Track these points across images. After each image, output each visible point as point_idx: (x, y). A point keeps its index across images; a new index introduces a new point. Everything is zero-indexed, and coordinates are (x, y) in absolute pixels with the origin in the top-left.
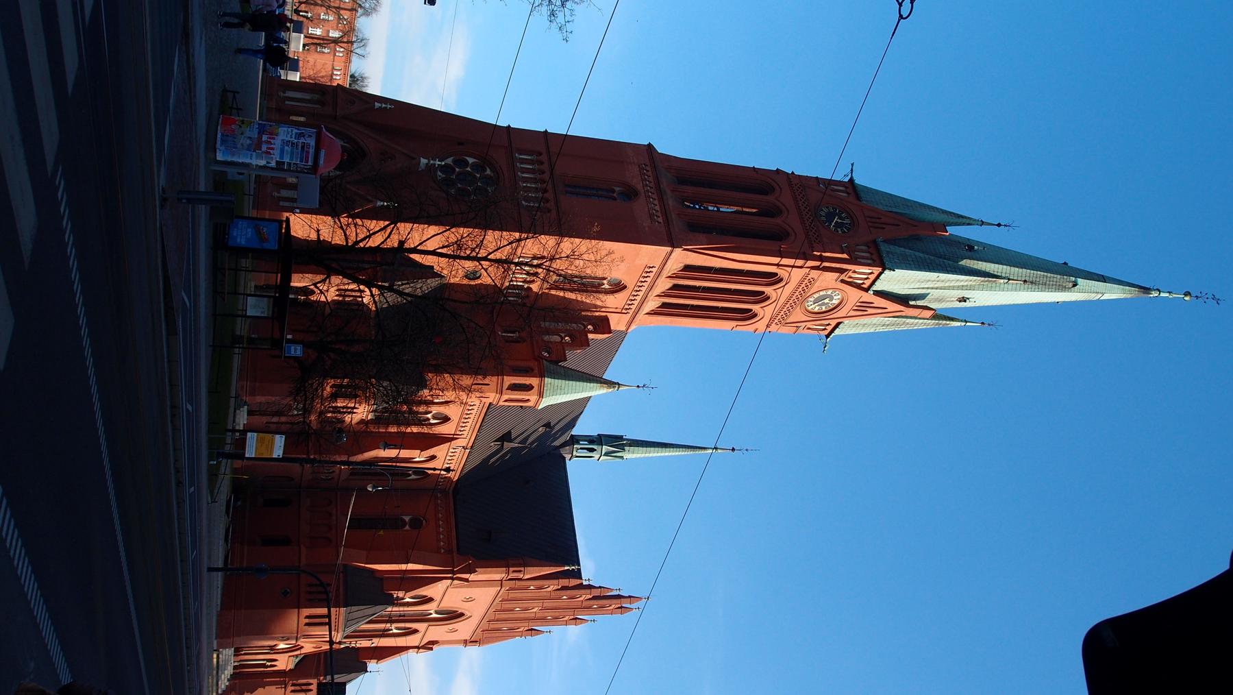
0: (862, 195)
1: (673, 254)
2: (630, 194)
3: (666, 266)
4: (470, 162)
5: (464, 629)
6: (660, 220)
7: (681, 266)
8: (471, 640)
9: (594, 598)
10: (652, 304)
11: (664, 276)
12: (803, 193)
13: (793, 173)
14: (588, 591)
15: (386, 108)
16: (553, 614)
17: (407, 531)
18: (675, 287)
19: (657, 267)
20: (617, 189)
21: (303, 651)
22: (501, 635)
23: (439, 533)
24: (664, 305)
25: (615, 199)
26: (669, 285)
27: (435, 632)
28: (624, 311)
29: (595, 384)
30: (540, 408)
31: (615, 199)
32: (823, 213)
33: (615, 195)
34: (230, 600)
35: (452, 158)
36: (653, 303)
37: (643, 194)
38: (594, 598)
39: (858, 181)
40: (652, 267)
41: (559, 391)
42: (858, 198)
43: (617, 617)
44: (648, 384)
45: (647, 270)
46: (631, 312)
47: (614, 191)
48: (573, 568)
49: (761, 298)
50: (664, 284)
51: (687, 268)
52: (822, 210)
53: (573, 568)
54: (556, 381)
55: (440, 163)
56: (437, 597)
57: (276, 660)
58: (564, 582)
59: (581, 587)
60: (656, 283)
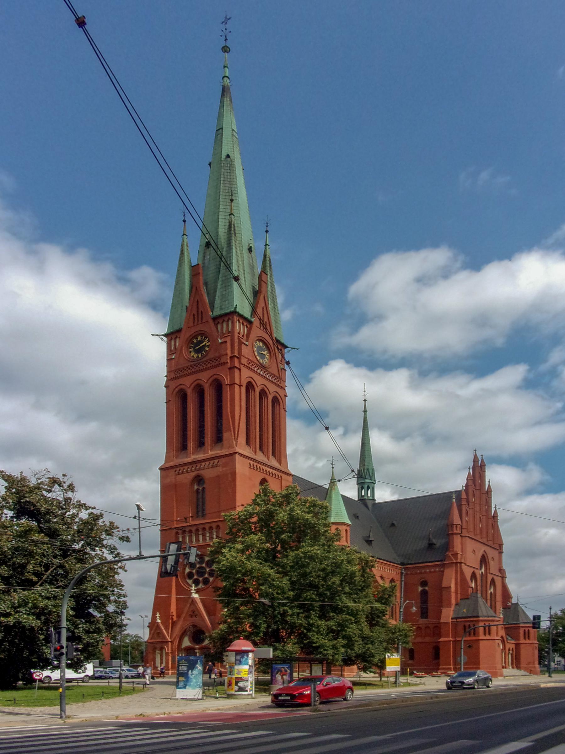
0: (176, 328)
1: (240, 452)
2: (199, 479)
3: (248, 456)
6: (216, 461)
7: (247, 447)
10: (275, 463)
11: (255, 456)
18: (261, 449)
19: (250, 461)
20: (196, 487)
24: (274, 454)
25: (203, 489)
26: (261, 453)
28: (280, 478)
29: (333, 493)
30: (351, 523)
31: (203, 489)
32: (195, 356)
33: (201, 488)
36: (273, 461)
37: (198, 472)
39: (165, 331)
40: (250, 464)
41: (339, 513)
42: (179, 331)
44: (331, 462)
45: (252, 467)
46: (280, 474)
47: (198, 490)
49: (263, 393)
50: (260, 457)
51: (248, 442)
52: (193, 356)
54: (332, 515)
60: (261, 461)
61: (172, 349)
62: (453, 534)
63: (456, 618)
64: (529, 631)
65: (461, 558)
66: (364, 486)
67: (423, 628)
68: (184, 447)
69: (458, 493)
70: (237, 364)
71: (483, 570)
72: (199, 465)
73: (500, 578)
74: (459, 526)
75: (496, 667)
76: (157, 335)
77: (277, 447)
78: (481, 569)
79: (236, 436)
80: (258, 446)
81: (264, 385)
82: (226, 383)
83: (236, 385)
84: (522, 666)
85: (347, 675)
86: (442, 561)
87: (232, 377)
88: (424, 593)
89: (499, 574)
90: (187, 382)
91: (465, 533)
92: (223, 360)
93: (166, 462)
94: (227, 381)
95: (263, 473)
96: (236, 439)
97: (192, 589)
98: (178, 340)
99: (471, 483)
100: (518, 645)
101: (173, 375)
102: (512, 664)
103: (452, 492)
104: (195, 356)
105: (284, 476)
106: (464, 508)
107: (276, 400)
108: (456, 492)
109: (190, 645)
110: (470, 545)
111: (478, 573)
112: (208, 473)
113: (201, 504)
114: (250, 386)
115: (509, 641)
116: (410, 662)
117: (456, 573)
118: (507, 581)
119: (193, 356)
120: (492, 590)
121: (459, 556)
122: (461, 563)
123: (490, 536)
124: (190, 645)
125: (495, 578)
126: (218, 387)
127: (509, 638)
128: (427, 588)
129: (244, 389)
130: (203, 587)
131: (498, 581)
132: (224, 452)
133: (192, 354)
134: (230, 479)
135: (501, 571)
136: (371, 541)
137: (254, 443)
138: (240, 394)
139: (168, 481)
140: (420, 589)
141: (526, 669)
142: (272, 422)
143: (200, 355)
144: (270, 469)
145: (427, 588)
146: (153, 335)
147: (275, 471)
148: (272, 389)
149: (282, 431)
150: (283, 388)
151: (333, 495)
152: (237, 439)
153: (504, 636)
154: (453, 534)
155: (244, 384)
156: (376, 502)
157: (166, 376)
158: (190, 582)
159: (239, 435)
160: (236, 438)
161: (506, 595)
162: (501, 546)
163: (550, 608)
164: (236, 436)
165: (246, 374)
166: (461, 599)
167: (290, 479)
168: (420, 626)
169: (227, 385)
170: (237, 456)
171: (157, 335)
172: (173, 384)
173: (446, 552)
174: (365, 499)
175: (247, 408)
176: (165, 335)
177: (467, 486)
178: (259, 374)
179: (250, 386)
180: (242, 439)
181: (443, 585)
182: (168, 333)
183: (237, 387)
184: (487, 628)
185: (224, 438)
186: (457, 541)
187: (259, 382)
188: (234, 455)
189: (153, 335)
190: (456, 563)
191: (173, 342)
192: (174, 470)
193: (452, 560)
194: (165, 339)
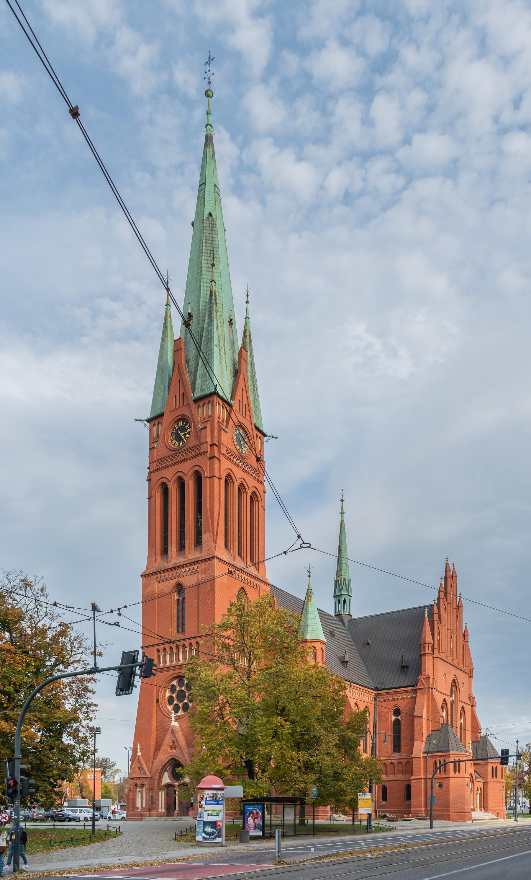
1: (219, 557)
2: (180, 588)
3: (227, 561)
4: (169, 695)
5: (462, 678)
6: (196, 567)
8: (469, 673)
9: (446, 596)
10: (252, 570)
11: (233, 561)
12: (163, 460)
13: (149, 468)
14: (442, 601)
15: (140, 749)
16: (455, 623)
17: (401, 718)
21: (473, 773)
22: (467, 655)
23: (402, 698)
26: (240, 559)
27: (464, 697)
28: (258, 588)
29: (309, 605)
31: (184, 599)
32: (177, 444)
33: (181, 599)
34: (445, 815)
35: (168, 706)
38: (446, 596)
39: (148, 416)
41: (315, 629)
42: (161, 415)
43: (459, 579)
44: (307, 570)
46: (258, 583)
47: (178, 600)
48: (426, 611)
49: (242, 488)
51: (226, 546)
52: (174, 445)
53: (426, 611)
54: (308, 631)
55: (173, 713)
56: (443, 697)
57: (478, 788)
58: (436, 617)
59: (438, 605)
61: (155, 436)
62: (425, 654)
63: (428, 753)
64: (496, 767)
65: (433, 683)
66: (340, 599)
67: (396, 764)
68: (165, 551)
69: (431, 607)
70: (216, 454)
71: (453, 698)
72: (179, 571)
73: (470, 707)
74: (431, 646)
75: (465, 809)
76: (140, 420)
77: (255, 551)
78: (451, 696)
79: (215, 537)
80: (237, 550)
81: (243, 478)
82: (206, 476)
83: (215, 478)
84: (490, 807)
85: (322, 818)
86: (414, 686)
87: (212, 469)
88: (397, 723)
89: (469, 702)
90: (170, 474)
91: (436, 654)
92: (203, 448)
93: (147, 568)
94: (207, 474)
95: (241, 581)
96: (215, 541)
97: (171, 716)
98: (160, 426)
99: (442, 595)
100: (486, 783)
101: (155, 467)
102: (480, 806)
103: (424, 607)
104: (177, 444)
105: (262, 585)
106: (436, 624)
107: (254, 497)
108: (428, 606)
109: (170, 781)
110: (441, 667)
111: (449, 700)
112: (188, 581)
113: (181, 617)
114: (228, 479)
115: (477, 780)
116: (384, 803)
117: (428, 697)
118: (477, 710)
119: (174, 445)
120: (462, 721)
121: (431, 680)
122: (432, 688)
123: (461, 657)
124: (170, 781)
125: (466, 707)
126: (199, 479)
127: (478, 776)
128: (399, 718)
129: (223, 482)
130: (182, 713)
131: (468, 709)
132: (204, 555)
133: (174, 441)
134: (209, 588)
135: (471, 698)
136: (347, 662)
137: (232, 546)
138: (219, 487)
139: (149, 589)
140: (393, 718)
141: (493, 811)
142: (251, 521)
143: (181, 443)
144: (248, 578)
145: (399, 718)
146: (136, 420)
147: (254, 580)
148: (251, 483)
149: (261, 534)
150: (261, 483)
151: (310, 608)
152: (216, 541)
153: (473, 773)
154: (425, 654)
155: (223, 477)
156: (353, 617)
157: (149, 468)
158: (170, 708)
159: (218, 537)
160: (215, 539)
161: (476, 727)
162: (471, 669)
163: (517, 742)
164: (215, 537)
165: (225, 464)
166: (432, 731)
167: (268, 589)
168: (393, 761)
169: (207, 477)
170: (216, 560)
171: (140, 420)
172: (156, 477)
173: (418, 677)
174: (341, 614)
175: (226, 505)
176: (149, 421)
177: (439, 599)
178: (238, 466)
179: (228, 479)
180: (221, 542)
181: (415, 714)
182: (150, 417)
183: (216, 480)
184: (457, 763)
185: (203, 540)
186: (428, 662)
187: (239, 475)
188: (213, 560)
189: (136, 420)
190: (428, 688)
191: (155, 428)
192: (156, 577)
193: (424, 685)
194: (148, 425)
